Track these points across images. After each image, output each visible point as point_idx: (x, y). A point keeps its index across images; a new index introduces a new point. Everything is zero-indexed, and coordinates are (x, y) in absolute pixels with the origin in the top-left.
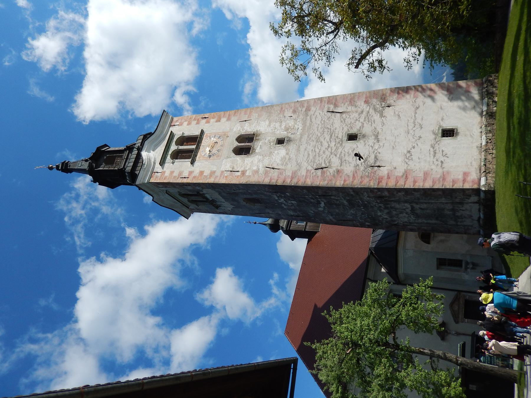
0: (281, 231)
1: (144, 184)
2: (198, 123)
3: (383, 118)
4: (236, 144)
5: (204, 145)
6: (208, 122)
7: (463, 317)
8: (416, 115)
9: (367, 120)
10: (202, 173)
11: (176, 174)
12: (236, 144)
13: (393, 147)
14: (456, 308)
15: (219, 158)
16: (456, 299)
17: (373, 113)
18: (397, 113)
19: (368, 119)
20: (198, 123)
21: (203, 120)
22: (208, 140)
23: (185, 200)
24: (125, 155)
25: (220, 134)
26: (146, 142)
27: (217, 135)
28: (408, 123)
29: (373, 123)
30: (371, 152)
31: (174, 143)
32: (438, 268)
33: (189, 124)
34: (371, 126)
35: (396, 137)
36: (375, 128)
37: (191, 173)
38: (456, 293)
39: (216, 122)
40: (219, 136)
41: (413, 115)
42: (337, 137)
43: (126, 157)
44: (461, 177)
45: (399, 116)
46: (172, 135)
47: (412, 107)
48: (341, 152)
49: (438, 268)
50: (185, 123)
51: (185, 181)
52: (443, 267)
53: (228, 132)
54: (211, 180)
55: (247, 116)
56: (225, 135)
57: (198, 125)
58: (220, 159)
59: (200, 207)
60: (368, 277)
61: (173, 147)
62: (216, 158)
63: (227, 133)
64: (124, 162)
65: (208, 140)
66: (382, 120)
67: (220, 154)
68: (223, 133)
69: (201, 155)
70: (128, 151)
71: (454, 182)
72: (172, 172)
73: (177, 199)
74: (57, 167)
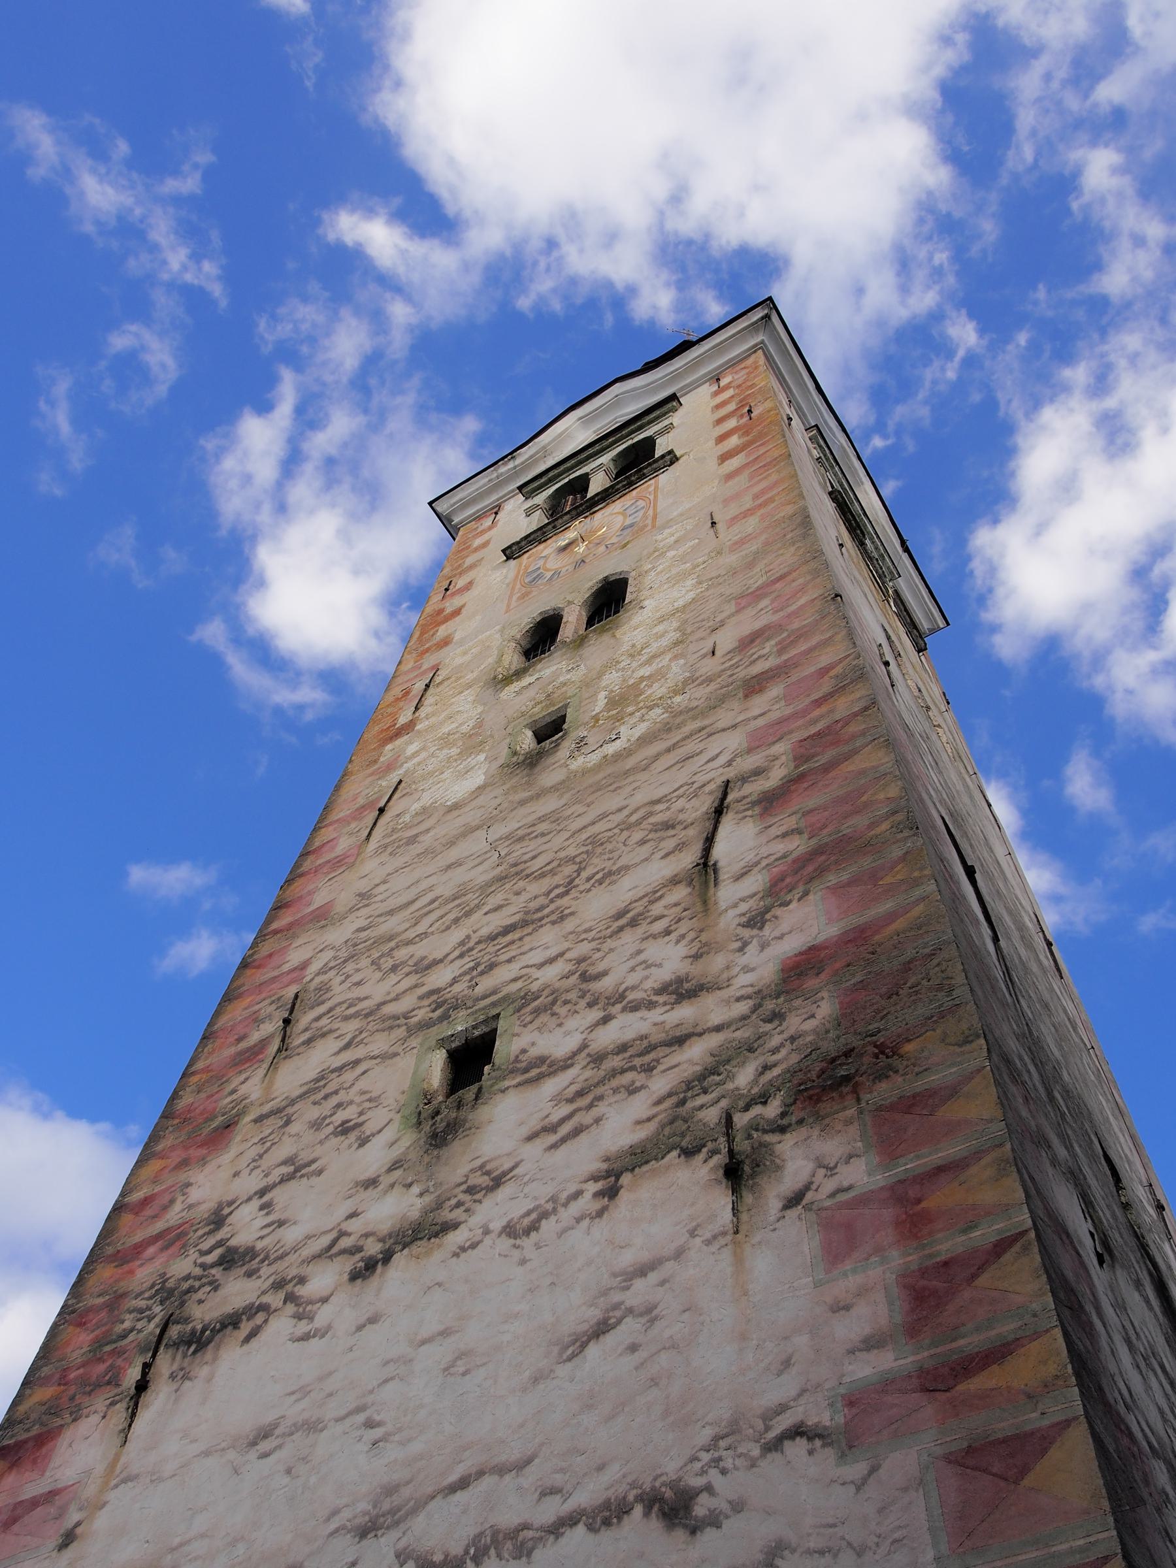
3: (593, 1187)
8: (581, 1529)
9: (602, 1073)
13: (266, 1437)
17: (660, 1084)
18: (641, 1291)
19: (614, 1073)
28: (488, 1481)
29: (553, 1138)
30: (280, 1266)
34: (530, 1138)
35: (361, 1418)
36: (497, 1182)
41: (585, 1497)
42: (492, 966)
45: (601, 1329)
47: (707, 1433)
48: (357, 1062)
66: (577, 1195)
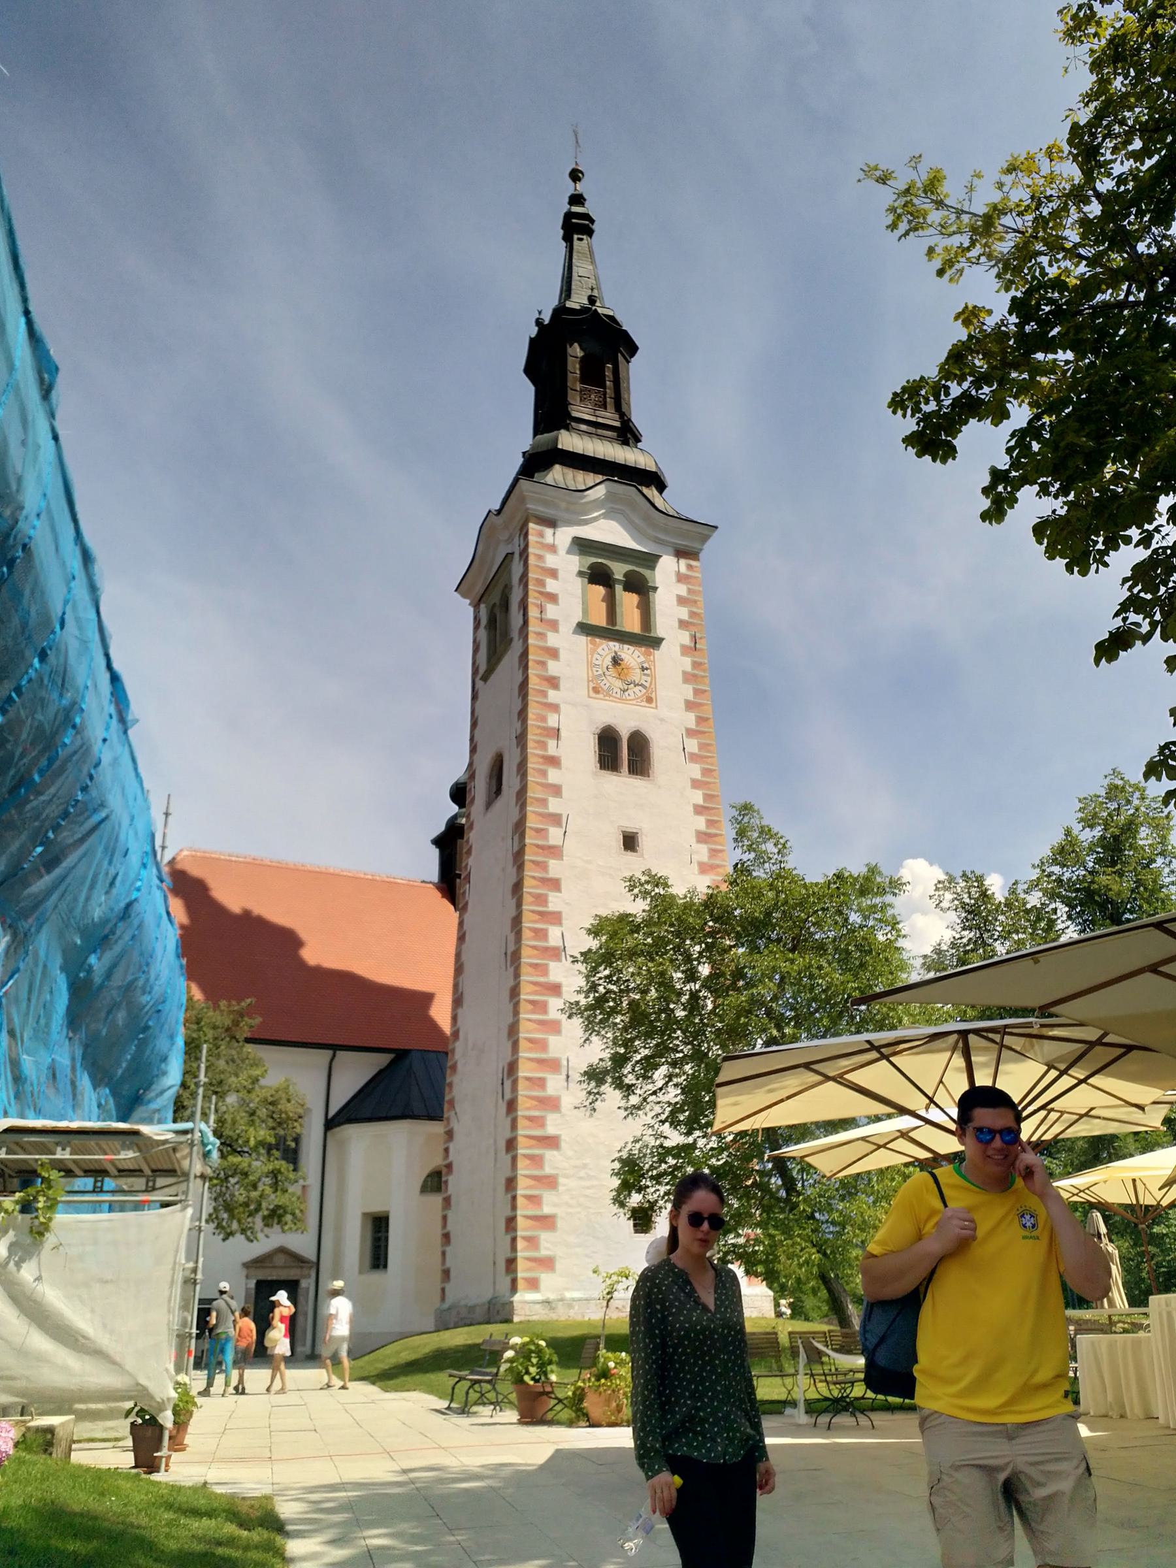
0: (455, 809)
1: (523, 500)
2: (683, 624)
4: (625, 735)
5: (625, 650)
6: (685, 650)
7: (260, 1278)
10: (554, 653)
11: (551, 586)
12: (625, 735)
14: (280, 1260)
15: (591, 692)
16: (298, 1260)
20: (683, 624)
21: (691, 635)
22: (636, 657)
23: (495, 597)
24: (609, 418)
25: (653, 686)
26: (634, 489)
27: (649, 679)
31: (628, 567)
32: (365, 1215)
33: (681, 601)
37: (554, 625)
38: (314, 1258)
39: (685, 673)
40: (647, 685)
43: (600, 420)
44: (544, 1252)
46: (650, 560)
49: (365, 1215)
50: (682, 590)
51: (533, 612)
52: (369, 1227)
53: (656, 707)
54: (534, 683)
55: (695, 750)
56: (649, 700)
57: (676, 624)
58: (589, 697)
59: (483, 634)
60: (338, 1052)
61: (619, 570)
62: (592, 685)
63: (653, 705)
64: (587, 417)
65: (636, 657)
67: (601, 696)
68: (653, 696)
69: (601, 644)
70: (617, 424)
71: (532, 1241)
72: (553, 573)
73: (491, 587)
74: (577, 199)
